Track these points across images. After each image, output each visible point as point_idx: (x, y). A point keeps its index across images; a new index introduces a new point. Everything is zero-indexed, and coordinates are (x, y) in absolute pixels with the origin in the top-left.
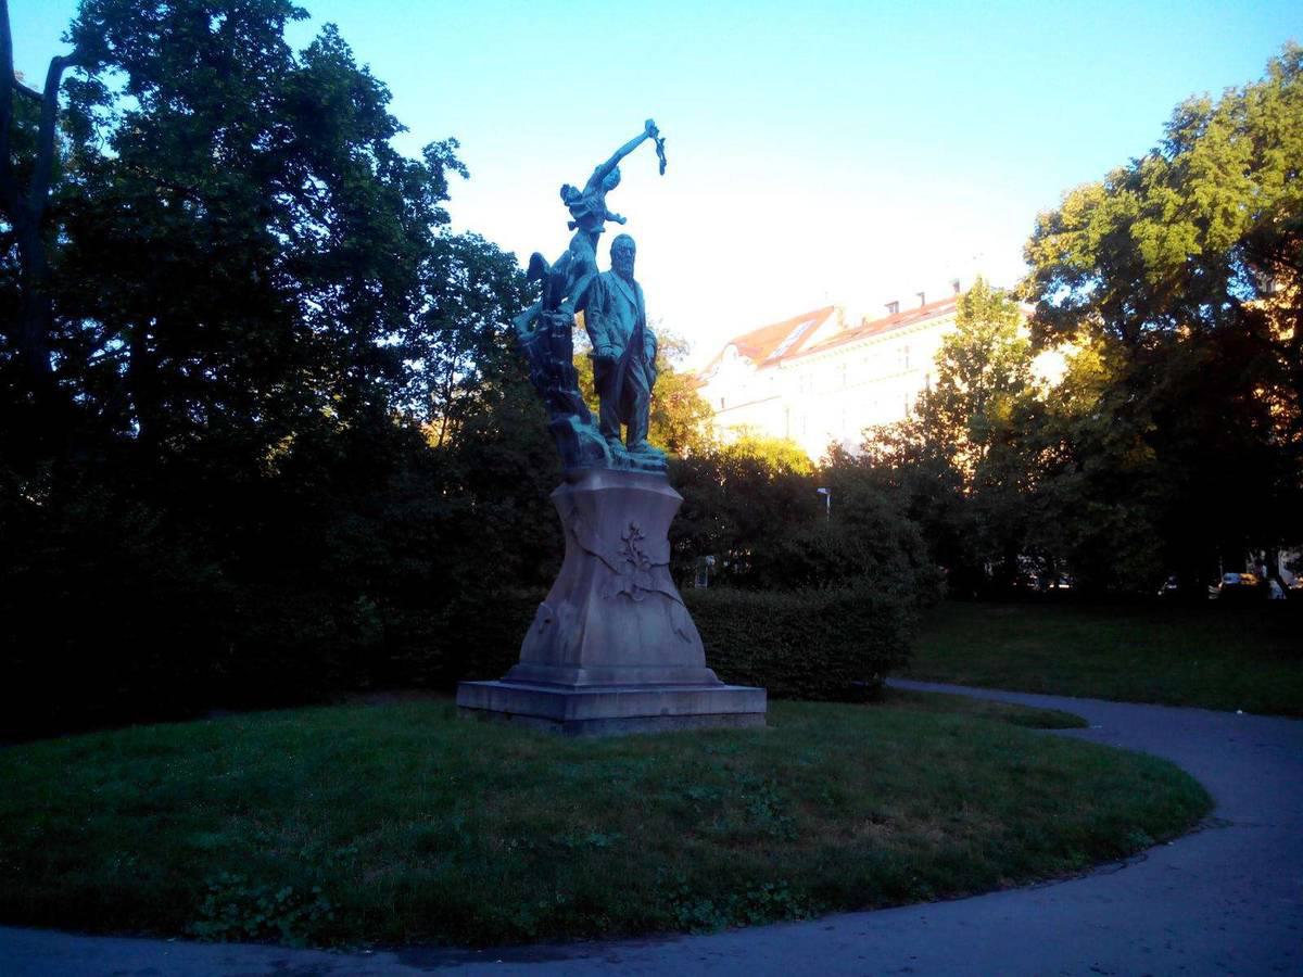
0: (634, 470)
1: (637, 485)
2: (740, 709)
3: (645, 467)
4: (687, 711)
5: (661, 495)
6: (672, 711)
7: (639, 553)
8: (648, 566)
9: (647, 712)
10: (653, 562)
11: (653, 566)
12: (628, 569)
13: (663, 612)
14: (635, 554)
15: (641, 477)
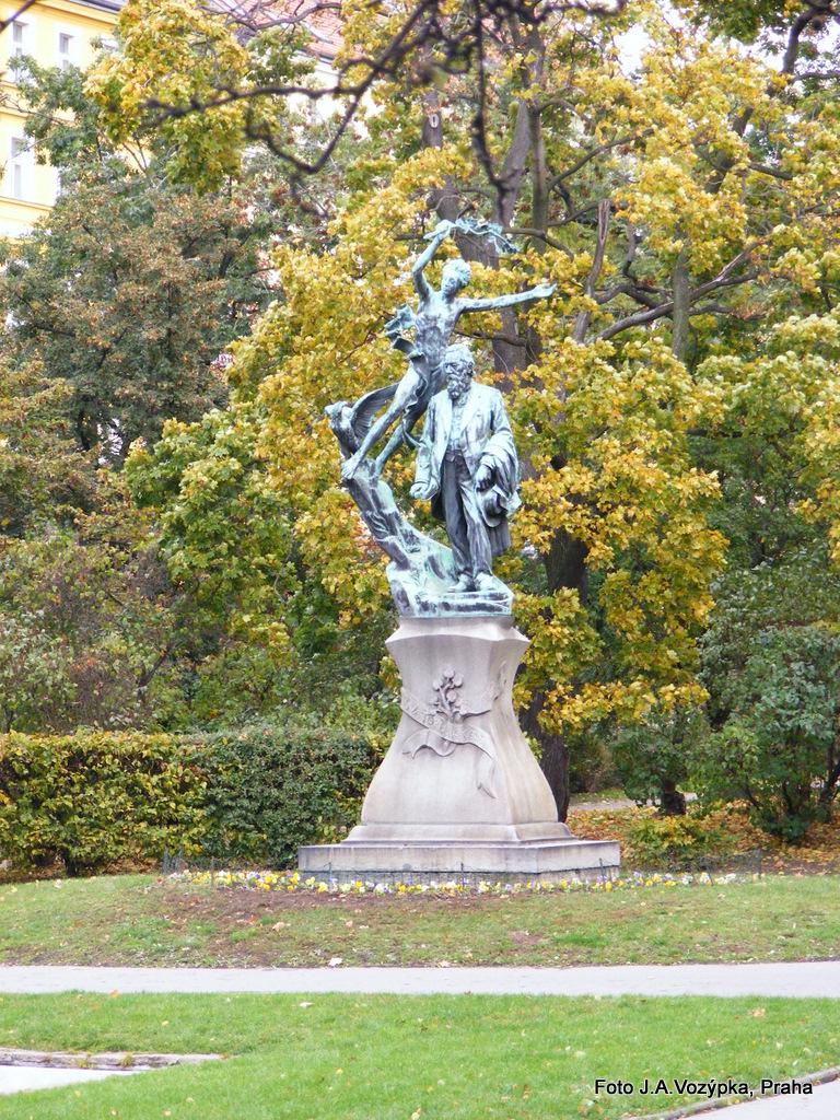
0: (452, 613)
1: (443, 631)
2: (501, 868)
3: (460, 608)
4: (435, 869)
5: (469, 638)
6: (416, 866)
7: (451, 704)
8: (458, 717)
9: (383, 867)
10: (463, 712)
11: (466, 717)
12: (438, 719)
13: (472, 764)
14: (446, 704)
15: (448, 622)
